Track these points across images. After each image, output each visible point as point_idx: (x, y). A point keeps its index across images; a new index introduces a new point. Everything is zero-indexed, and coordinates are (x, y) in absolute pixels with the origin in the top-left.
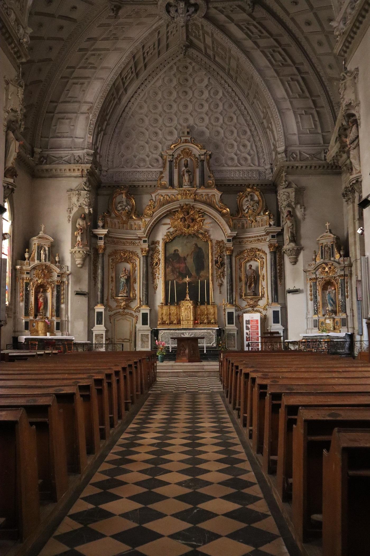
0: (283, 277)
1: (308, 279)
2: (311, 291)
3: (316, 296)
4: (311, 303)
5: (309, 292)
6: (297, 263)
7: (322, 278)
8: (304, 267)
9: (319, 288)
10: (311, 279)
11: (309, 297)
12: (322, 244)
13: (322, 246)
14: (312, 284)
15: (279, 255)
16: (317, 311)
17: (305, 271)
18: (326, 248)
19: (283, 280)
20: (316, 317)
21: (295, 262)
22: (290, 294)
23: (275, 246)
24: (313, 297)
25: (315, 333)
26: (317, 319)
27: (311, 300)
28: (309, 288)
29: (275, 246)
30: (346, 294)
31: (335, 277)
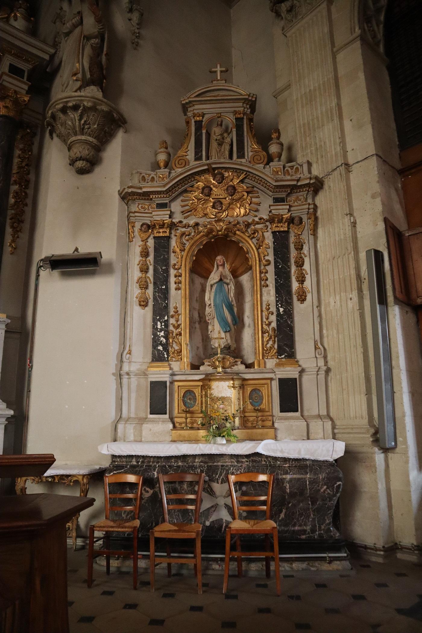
0: (26, 226)
1: (138, 225)
2: (144, 270)
3: (167, 290)
4: (141, 318)
5: (136, 274)
6: (98, 170)
7: (197, 224)
8: (122, 183)
9: (179, 259)
10: (148, 227)
11: (135, 291)
12: (203, 115)
13: (199, 125)
14: (151, 243)
15: (23, 150)
16: (166, 347)
17: (126, 197)
18: (216, 131)
19: (24, 237)
20: (160, 373)
21: (87, 164)
22: (56, 273)
23: (16, 102)
24: (150, 292)
25: (158, 441)
26: (166, 378)
27: (143, 304)
28: (136, 259)
29: (16, 102)
30: (295, 285)
31: (248, 225)
